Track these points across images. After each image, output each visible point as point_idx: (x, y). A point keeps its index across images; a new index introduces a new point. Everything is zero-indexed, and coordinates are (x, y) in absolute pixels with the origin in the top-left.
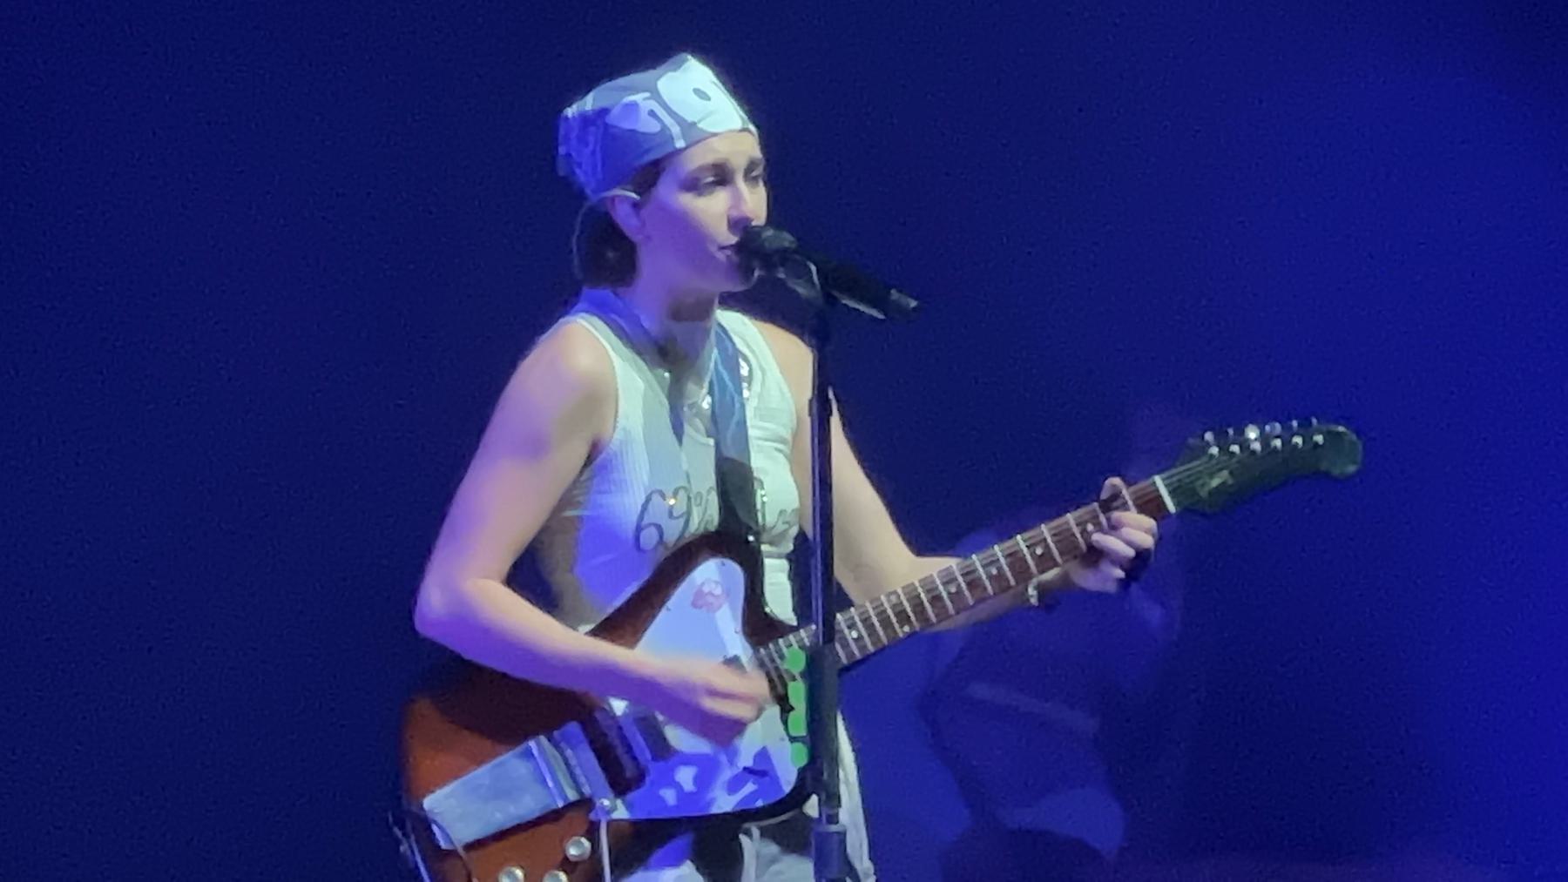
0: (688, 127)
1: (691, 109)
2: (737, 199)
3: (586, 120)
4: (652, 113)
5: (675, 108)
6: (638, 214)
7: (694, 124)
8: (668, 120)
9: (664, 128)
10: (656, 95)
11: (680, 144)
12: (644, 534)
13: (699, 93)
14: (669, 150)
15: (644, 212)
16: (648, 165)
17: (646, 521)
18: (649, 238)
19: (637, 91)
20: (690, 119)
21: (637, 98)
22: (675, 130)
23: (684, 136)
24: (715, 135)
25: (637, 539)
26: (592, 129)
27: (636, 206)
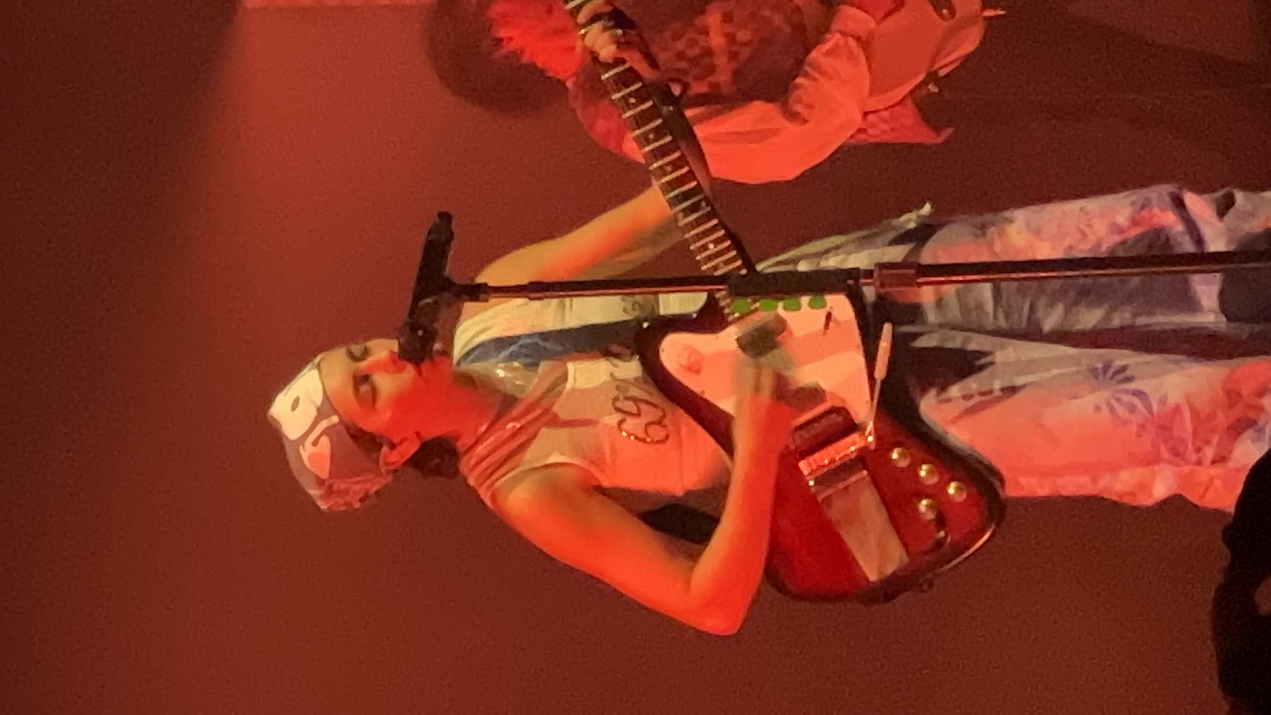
0: (321, 414)
1: (307, 413)
2: (378, 366)
3: (330, 492)
4: (315, 443)
6: (401, 443)
7: (318, 410)
9: (324, 432)
11: (335, 419)
13: (295, 406)
14: (341, 427)
16: (358, 441)
19: (300, 457)
20: (314, 413)
22: (324, 424)
26: (335, 487)
27: (393, 447)
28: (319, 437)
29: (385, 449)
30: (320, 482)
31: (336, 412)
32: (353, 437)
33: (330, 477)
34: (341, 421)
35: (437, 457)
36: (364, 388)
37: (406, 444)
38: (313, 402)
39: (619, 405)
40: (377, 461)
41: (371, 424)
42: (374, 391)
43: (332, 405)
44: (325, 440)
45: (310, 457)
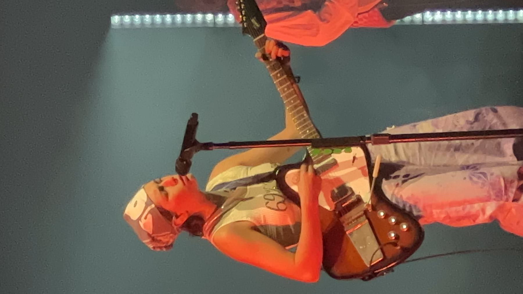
1: (141, 206)
3: (153, 240)
4: (146, 218)
6: (180, 216)
9: (150, 212)
10: (139, 219)
11: (153, 206)
12: (280, 208)
15: (178, 214)
17: (277, 208)
18: (187, 212)
21: (141, 224)
22: (149, 209)
24: (147, 195)
25: (282, 210)
26: (155, 238)
27: (177, 217)
29: (174, 218)
30: (149, 234)
31: (153, 203)
32: (161, 213)
34: (156, 206)
38: (143, 200)
39: (266, 197)
40: (171, 225)
41: (167, 207)
42: (167, 195)
43: (152, 201)
44: (150, 216)
45: (145, 225)
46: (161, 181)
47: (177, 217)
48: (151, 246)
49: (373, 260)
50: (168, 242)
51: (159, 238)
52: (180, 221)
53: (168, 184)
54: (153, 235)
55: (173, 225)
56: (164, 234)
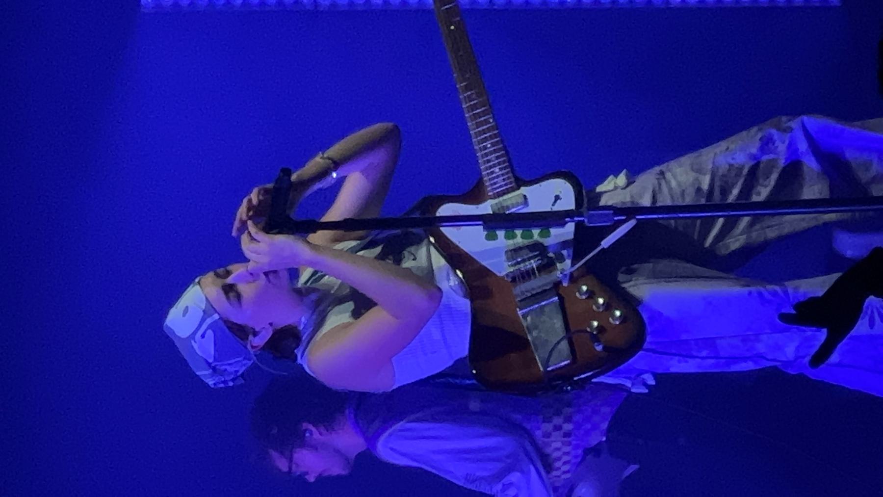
0: (206, 314)
3: (214, 369)
4: (203, 336)
5: (198, 323)
7: (204, 311)
8: (204, 326)
9: (210, 327)
11: (216, 316)
14: (220, 322)
15: (257, 330)
16: (232, 333)
18: (271, 324)
20: (202, 314)
22: (209, 321)
23: (212, 315)
24: (207, 299)
28: (206, 331)
29: (251, 337)
30: (209, 364)
31: (216, 312)
32: (229, 328)
33: (215, 360)
34: (221, 318)
35: (286, 341)
36: (231, 295)
37: (264, 332)
40: (246, 347)
42: (239, 296)
44: (210, 333)
46: (228, 273)
47: (255, 334)
48: (211, 382)
49: (550, 363)
50: (237, 371)
51: (223, 367)
52: (259, 341)
53: (240, 278)
54: (213, 365)
55: (249, 347)
56: (233, 361)
